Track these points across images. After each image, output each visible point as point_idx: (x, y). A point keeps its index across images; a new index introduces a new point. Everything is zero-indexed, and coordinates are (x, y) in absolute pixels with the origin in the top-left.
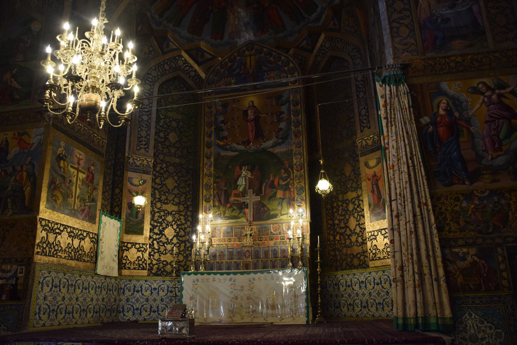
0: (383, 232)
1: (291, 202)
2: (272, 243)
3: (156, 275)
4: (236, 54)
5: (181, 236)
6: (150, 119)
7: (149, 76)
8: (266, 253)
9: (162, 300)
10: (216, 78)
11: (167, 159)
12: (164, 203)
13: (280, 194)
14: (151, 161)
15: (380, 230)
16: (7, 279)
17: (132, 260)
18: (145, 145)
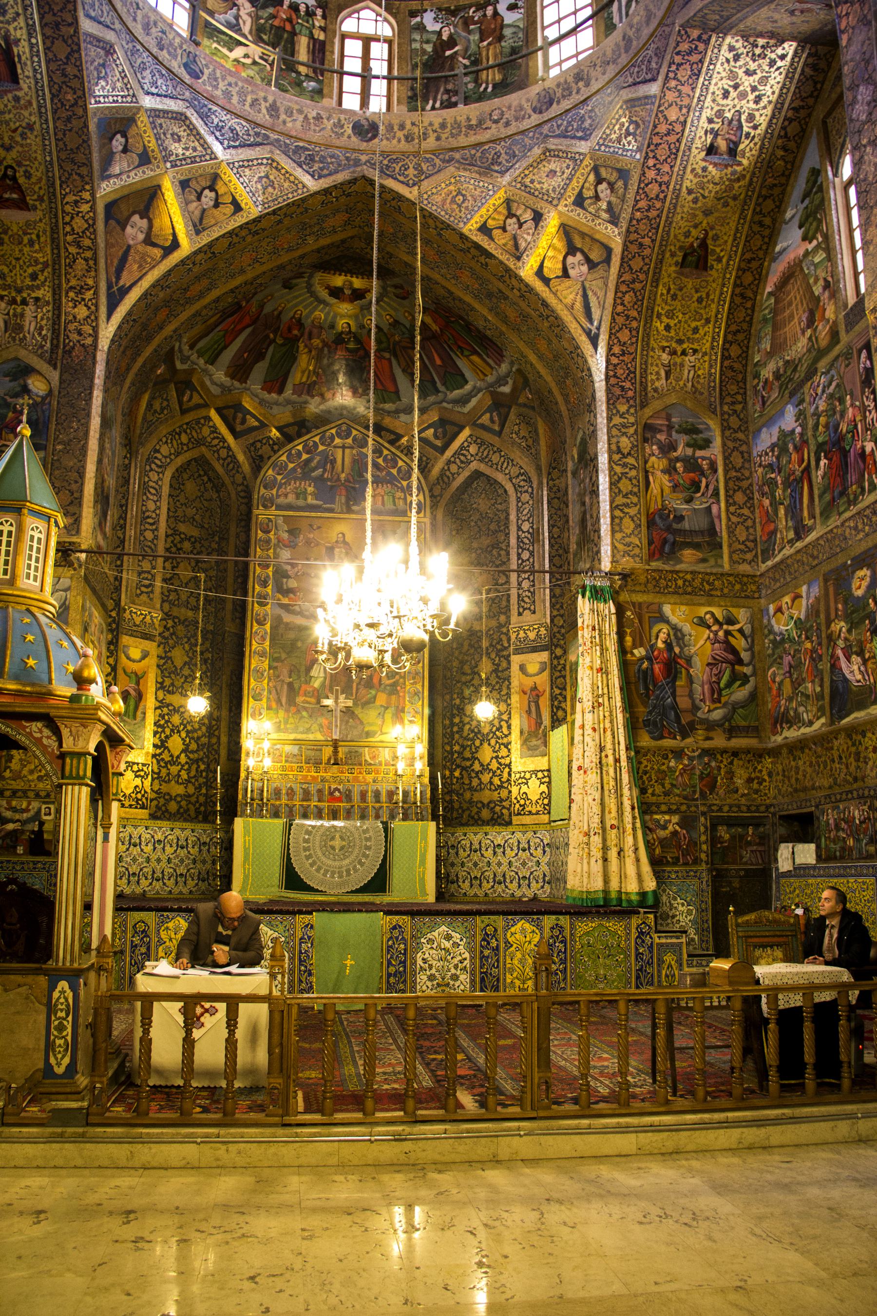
0: (540, 775)
1: (399, 714)
2: (369, 778)
3: (153, 817)
4: (317, 439)
5: (192, 752)
6: (156, 537)
7: (159, 455)
8: (363, 795)
9: (169, 861)
10: (279, 478)
11: (175, 612)
12: (169, 692)
13: (382, 699)
14: (157, 615)
15: (535, 772)
16: (24, 823)
17: (128, 792)
18: (147, 587)
